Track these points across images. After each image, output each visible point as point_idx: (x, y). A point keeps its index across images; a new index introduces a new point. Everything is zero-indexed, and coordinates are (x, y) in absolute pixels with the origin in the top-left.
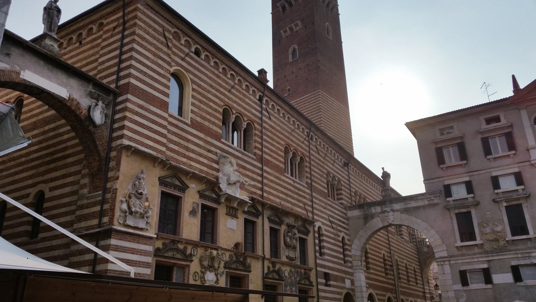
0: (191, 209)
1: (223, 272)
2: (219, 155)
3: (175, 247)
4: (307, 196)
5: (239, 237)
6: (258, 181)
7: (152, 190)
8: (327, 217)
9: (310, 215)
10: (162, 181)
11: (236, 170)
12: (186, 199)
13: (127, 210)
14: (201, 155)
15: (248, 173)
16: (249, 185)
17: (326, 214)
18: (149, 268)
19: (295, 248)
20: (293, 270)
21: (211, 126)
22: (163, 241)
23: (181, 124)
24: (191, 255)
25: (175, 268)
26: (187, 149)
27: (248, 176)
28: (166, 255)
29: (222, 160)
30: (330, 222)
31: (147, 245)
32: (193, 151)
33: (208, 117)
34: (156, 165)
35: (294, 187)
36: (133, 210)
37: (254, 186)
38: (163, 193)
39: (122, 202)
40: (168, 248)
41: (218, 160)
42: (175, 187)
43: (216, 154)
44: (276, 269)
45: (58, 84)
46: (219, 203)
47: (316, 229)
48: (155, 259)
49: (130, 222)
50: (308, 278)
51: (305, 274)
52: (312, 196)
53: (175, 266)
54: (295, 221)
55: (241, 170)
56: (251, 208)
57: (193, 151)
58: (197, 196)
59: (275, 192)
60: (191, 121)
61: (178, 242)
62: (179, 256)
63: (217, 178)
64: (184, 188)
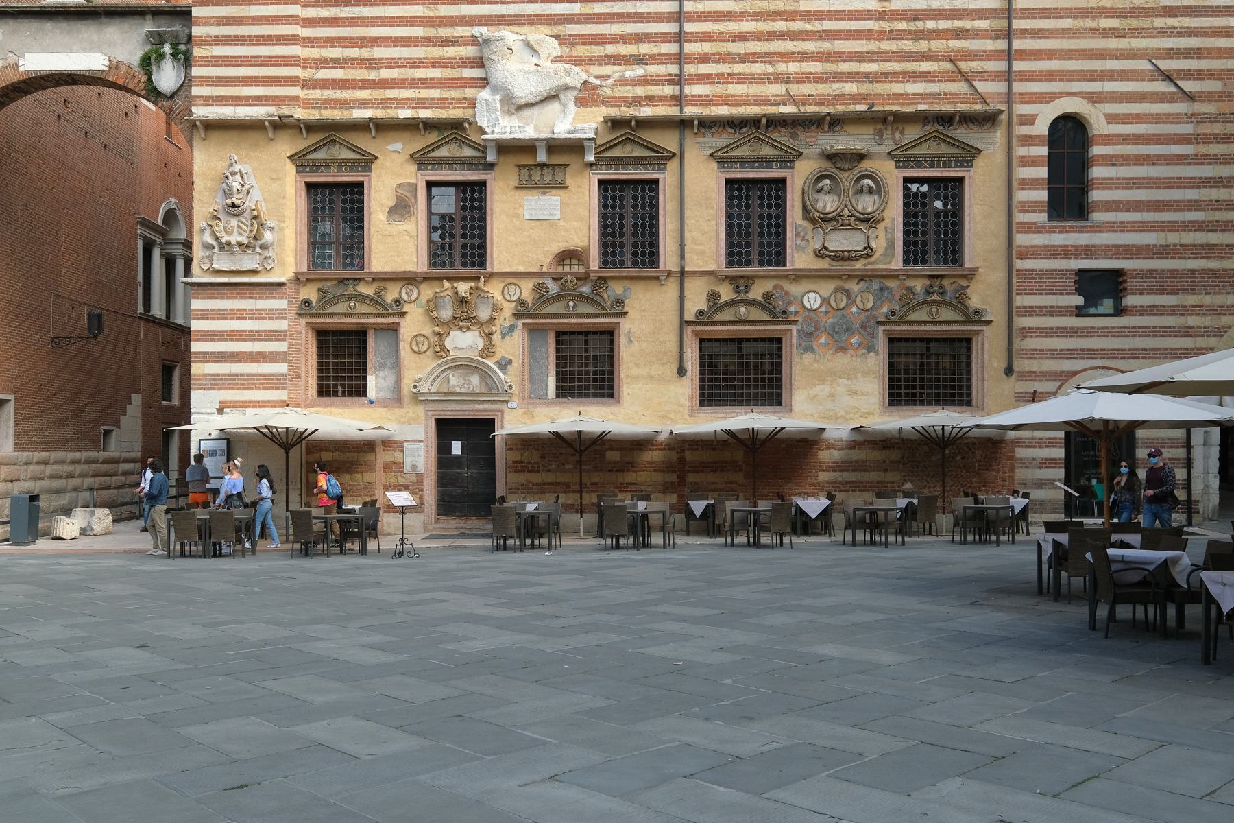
0: (392, 203)
1: (512, 328)
3: (351, 290)
4: (984, 24)
7: (274, 189)
8: (1144, 65)
10: (301, 161)
12: (373, 183)
13: (214, 243)
14: (417, 63)
15: (610, 49)
16: (621, 82)
17: (1131, 54)
20: (854, 287)
22: (319, 285)
24: (398, 302)
26: (371, 64)
27: (615, 60)
30: (1167, 77)
32: (391, 63)
34: (270, 135)
36: (223, 240)
38: (309, 186)
39: (203, 230)
40: (330, 295)
42: (340, 164)
43: (474, 40)
44: (756, 292)
45: (85, 50)
46: (491, 166)
47: (1041, 128)
48: (303, 321)
49: (223, 263)
50: (959, 303)
51: (928, 293)
54: (880, 133)
55: (582, 50)
56: (628, 147)
57: (391, 63)
58: (413, 168)
59: (758, 68)
61: (358, 280)
64: (366, 162)
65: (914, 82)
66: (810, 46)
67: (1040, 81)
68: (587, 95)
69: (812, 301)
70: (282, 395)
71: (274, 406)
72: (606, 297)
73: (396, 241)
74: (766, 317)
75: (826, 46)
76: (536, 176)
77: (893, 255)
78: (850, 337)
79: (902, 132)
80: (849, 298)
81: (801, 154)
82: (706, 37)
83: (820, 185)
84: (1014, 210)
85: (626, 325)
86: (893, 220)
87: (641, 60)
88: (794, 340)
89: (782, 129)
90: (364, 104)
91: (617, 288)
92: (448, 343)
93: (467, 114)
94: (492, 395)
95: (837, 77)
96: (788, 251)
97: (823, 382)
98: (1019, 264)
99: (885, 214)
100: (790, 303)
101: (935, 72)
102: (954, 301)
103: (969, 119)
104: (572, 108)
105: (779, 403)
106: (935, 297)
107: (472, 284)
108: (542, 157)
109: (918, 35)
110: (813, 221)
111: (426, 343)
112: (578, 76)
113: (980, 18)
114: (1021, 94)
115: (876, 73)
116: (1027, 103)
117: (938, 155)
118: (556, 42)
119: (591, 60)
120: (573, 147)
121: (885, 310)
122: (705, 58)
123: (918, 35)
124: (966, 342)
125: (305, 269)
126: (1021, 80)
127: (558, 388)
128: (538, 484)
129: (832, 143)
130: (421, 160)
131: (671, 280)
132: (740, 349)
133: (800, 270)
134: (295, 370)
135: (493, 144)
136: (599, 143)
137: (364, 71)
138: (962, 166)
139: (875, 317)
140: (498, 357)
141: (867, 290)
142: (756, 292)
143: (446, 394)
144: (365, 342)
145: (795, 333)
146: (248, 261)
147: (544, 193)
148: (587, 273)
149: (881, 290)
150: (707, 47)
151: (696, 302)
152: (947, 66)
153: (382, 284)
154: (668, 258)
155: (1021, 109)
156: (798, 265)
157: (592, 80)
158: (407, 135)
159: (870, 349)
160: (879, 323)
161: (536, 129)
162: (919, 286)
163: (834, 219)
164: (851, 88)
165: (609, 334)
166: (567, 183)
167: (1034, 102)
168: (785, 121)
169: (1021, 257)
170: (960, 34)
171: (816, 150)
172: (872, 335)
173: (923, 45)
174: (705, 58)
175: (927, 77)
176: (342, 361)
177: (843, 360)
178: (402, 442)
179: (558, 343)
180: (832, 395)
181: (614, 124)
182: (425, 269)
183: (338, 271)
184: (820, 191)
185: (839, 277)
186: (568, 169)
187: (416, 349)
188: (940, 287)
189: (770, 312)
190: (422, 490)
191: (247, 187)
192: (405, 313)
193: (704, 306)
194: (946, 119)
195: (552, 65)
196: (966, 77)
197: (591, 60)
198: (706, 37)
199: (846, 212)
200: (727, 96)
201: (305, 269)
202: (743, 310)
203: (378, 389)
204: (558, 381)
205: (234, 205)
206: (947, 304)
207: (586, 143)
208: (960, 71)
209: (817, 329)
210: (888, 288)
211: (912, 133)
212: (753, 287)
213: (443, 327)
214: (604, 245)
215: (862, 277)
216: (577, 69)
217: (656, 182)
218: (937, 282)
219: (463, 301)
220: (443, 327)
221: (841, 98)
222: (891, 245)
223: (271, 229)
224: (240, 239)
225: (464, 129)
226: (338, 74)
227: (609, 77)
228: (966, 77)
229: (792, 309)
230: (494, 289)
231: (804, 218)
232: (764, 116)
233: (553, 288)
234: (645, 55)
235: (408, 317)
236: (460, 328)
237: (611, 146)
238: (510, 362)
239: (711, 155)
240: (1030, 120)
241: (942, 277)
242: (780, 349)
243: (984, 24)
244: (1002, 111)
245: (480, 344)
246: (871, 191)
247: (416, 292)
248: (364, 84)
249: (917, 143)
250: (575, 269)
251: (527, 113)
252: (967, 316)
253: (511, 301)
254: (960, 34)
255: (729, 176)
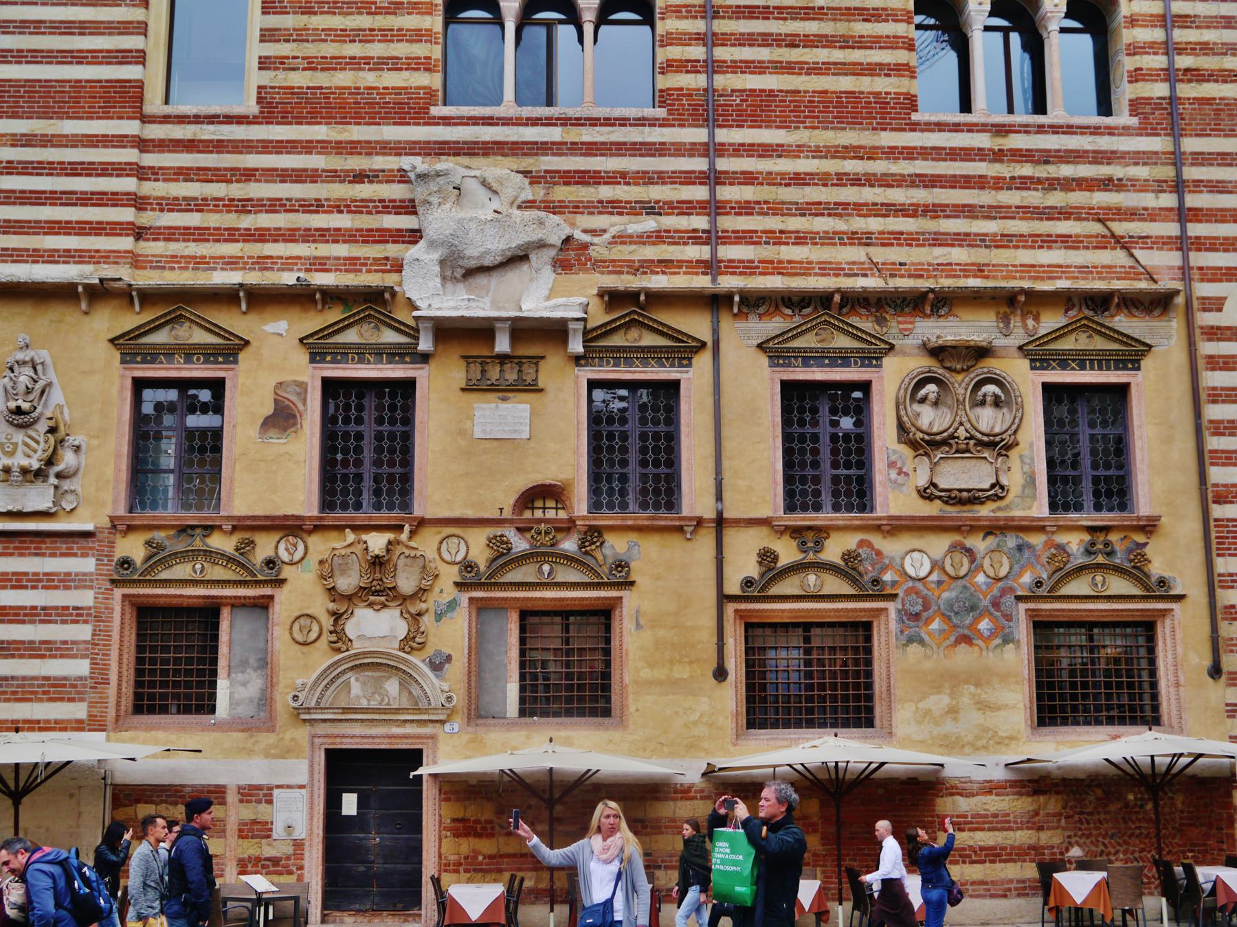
0: (269, 409)
1: (452, 605)
2: (412, 176)
3: (198, 544)
4: (1142, 172)
5: (567, 460)
6: (685, 208)
9: (1164, 261)
10: (128, 346)
11: (528, 205)
14: (316, 206)
15: (606, 192)
16: (622, 239)
18: (86, 622)
19: (999, 446)
20: (979, 544)
21: (369, 78)
22: (148, 536)
23: (211, 128)
24: (270, 563)
25: (225, 613)
26: (244, 206)
27: (614, 207)
28: (164, 575)
29: (420, 193)
31: (75, 555)
32: (275, 206)
33: (354, 50)
35: (998, 156)
37: (658, 237)
41: (408, 196)
42: (190, 352)
43: (402, 177)
44: (833, 551)
46: (425, 358)
48: (118, 593)
50: (1136, 570)
51: (1088, 552)
52: (1177, 159)
53: (226, 605)
54: (1006, 319)
55: (562, 193)
56: (634, 333)
57: (275, 206)
58: (303, 357)
60: (260, 100)
61: (209, 529)
62: (218, 572)
63: (398, 267)
64: (231, 349)
65: (1049, 248)
66: (898, 195)
67: (1226, 250)
68: (570, 255)
69: (917, 566)
70: (79, 711)
71: (64, 729)
72: (600, 558)
73: (272, 470)
74: (847, 589)
75: (921, 196)
76: (494, 373)
77: (1034, 497)
78: (977, 620)
79: (1037, 318)
80: (972, 561)
81: (892, 347)
82: (749, 178)
83: (923, 392)
84: (1206, 433)
85: (630, 601)
86: (1031, 445)
87: (652, 209)
88: (893, 625)
89: (863, 312)
90: (232, 263)
91: (616, 545)
92: (351, 628)
93: (390, 280)
94: (419, 711)
95: (939, 240)
96: (879, 489)
97: (938, 689)
98: (1218, 511)
99: (1020, 437)
100: (885, 569)
101: (1077, 236)
102: (1127, 565)
103: (1134, 303)
104: (547, 276)
105: (870, 723)
106: (1100, 559)
107: (389, 536)
108: (503, 344)
109: (1052, 184)
110: (914, 445)
111: (316, 628)
112: (556, 228)
113: (1136, 164)
114: (1201, 269)
115: (995, 235)
116: (1209, 281)
117: (1084, 352)
118: (527, 181)
119: (577, 208)
120: (554, 331)
121: (1027, 578)
122: (745, 208)
123: (1052, 184)
124: (1147, 628)
125: (121, 511)
126: (1199, 250)
127: (522, 700)
128: (491, 857)
129: (938, 332)
130: (318, 348)
131: (703, 532)
132: (807, 640)
133: (899, 518)
134: (99, 669)
135: (429, 325)
136: (590, 325)
137: (233, 215)
138: (1125, 368)
139: (1012, 589)
140: (429, 651)
141: (997, 550)
142: (833, 551)
143: (346, 710)
144: (216, 626)
145: (893, 614)
146: (38, 497)
147: (504, 399)
148: (572, 521)
149: (1020, 548)
150: (747, 193)
151: (743, 564)
152: (1097, 228)
153: (247, 535)
154: (696, 497)
155: (1204, 289)
156: (894, 511)
157: (579, 235)
158: (295, 312)
159: (1007, 640)
160: (1019, 598)
161: (495, 304)
162: (1074, 542)
163: (944, 442)
164: (958, 255)
165: (604, 614)
166: (541, 385)
167: (1221, 281)
168: (866, 299)
169: (1221, 499)
170: (1107, 184)
171: (913, 341)
172: (1009, 617)
173: (1057, 199)
174: (745, 208)
175: (1067, 241)
176: (173, 661)
177: (964, 656)
178: (271, 789)
179: (523, 629)
180: (953, 711)
181: (613, 298)
182: (315, 512)
183: (170, 512)
184: (923, 400)
185: (957, 529)
186: (542, 363)
187: (300, 638)
188: (1107, 544)
189: (854, 581)
190: (301, 868)
191: (41, 384)
192: (283, 581)
193: (753, 571)
194: (1101, 302)
195: (517, 212)
196: (1123, 243)
197: (577, 208)
198: (749, 178)
199: (962, 433)
200: (780, 262)
201: (121, 511)
202: (812, 578)
203: (233, 703)
204: (522, 689)
205: (18, 411)
206: (1119, 570)
207: (571, 325)
208: (1113, 236)
209: (926, 607)
210: (1030, 546)
211: (1051, 321)
212: (827, 543)
213: (343, 603)
214: (595, 477)
215: (993, 529)
216: (556, 219)
217: (675, 385)
218: (1101, 538)
219: (377, 563)
220: (343, 603)
221: (947, 268)
222: (1031, 481)
223: (77, 449)
224: (25, 462)
225: (384, 303)
226: (193, 219)
227: (605, 231)
228: (1123, 243)
229: (887, 577)
230: (427, 543)
231: (900, 442)
232: (838, 290)
233: (520, 544)
234: (657, 202)
235: (286, 588)
236: (371, 605)
237: (607, 330)
238: (449, 658)
239: (760, 346)
240: (1217, 304)
241: (1106, 529)
242: (869, 639)
243: (1142, 172)
244: (1177, 292)
245: (402, 629)
246: (997, 403)
247: (301, 547)
248: (232, 235)
249: (1059, 334)
250: (551, 514)
251: (481, 280)
252: (1146, 587)
253: (454, 563)
254: (1107, 184)
255: (786, 377)
